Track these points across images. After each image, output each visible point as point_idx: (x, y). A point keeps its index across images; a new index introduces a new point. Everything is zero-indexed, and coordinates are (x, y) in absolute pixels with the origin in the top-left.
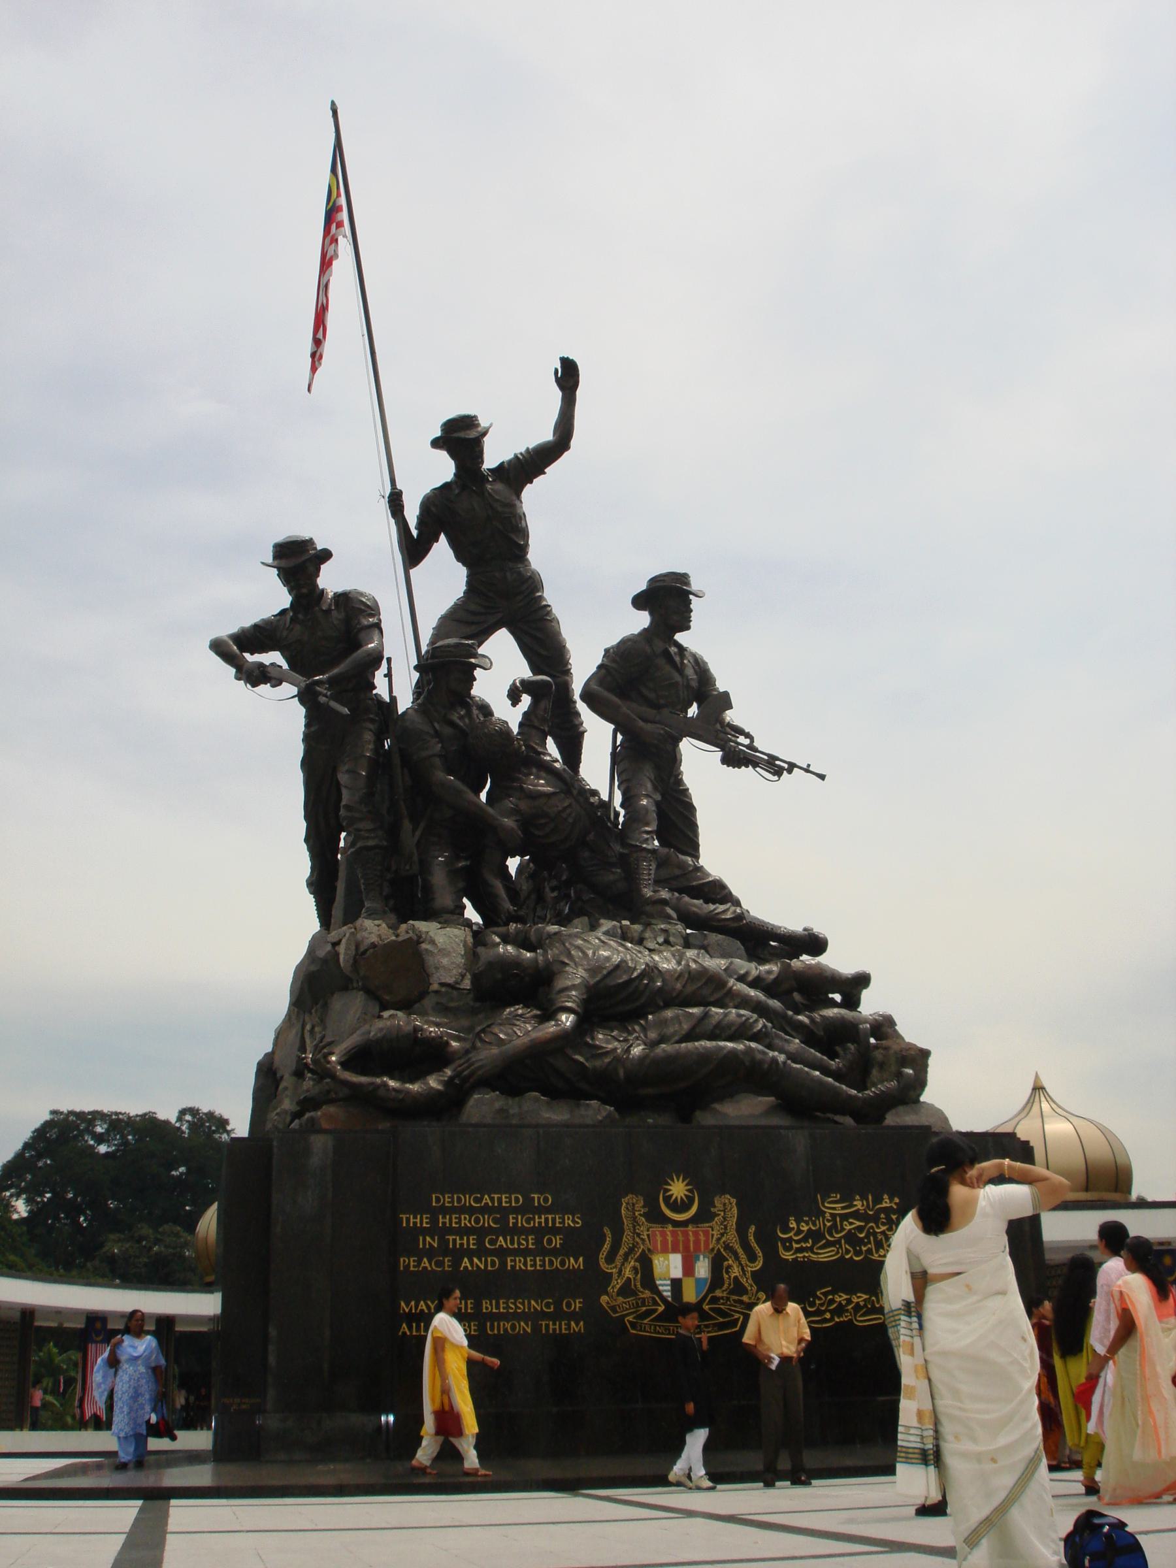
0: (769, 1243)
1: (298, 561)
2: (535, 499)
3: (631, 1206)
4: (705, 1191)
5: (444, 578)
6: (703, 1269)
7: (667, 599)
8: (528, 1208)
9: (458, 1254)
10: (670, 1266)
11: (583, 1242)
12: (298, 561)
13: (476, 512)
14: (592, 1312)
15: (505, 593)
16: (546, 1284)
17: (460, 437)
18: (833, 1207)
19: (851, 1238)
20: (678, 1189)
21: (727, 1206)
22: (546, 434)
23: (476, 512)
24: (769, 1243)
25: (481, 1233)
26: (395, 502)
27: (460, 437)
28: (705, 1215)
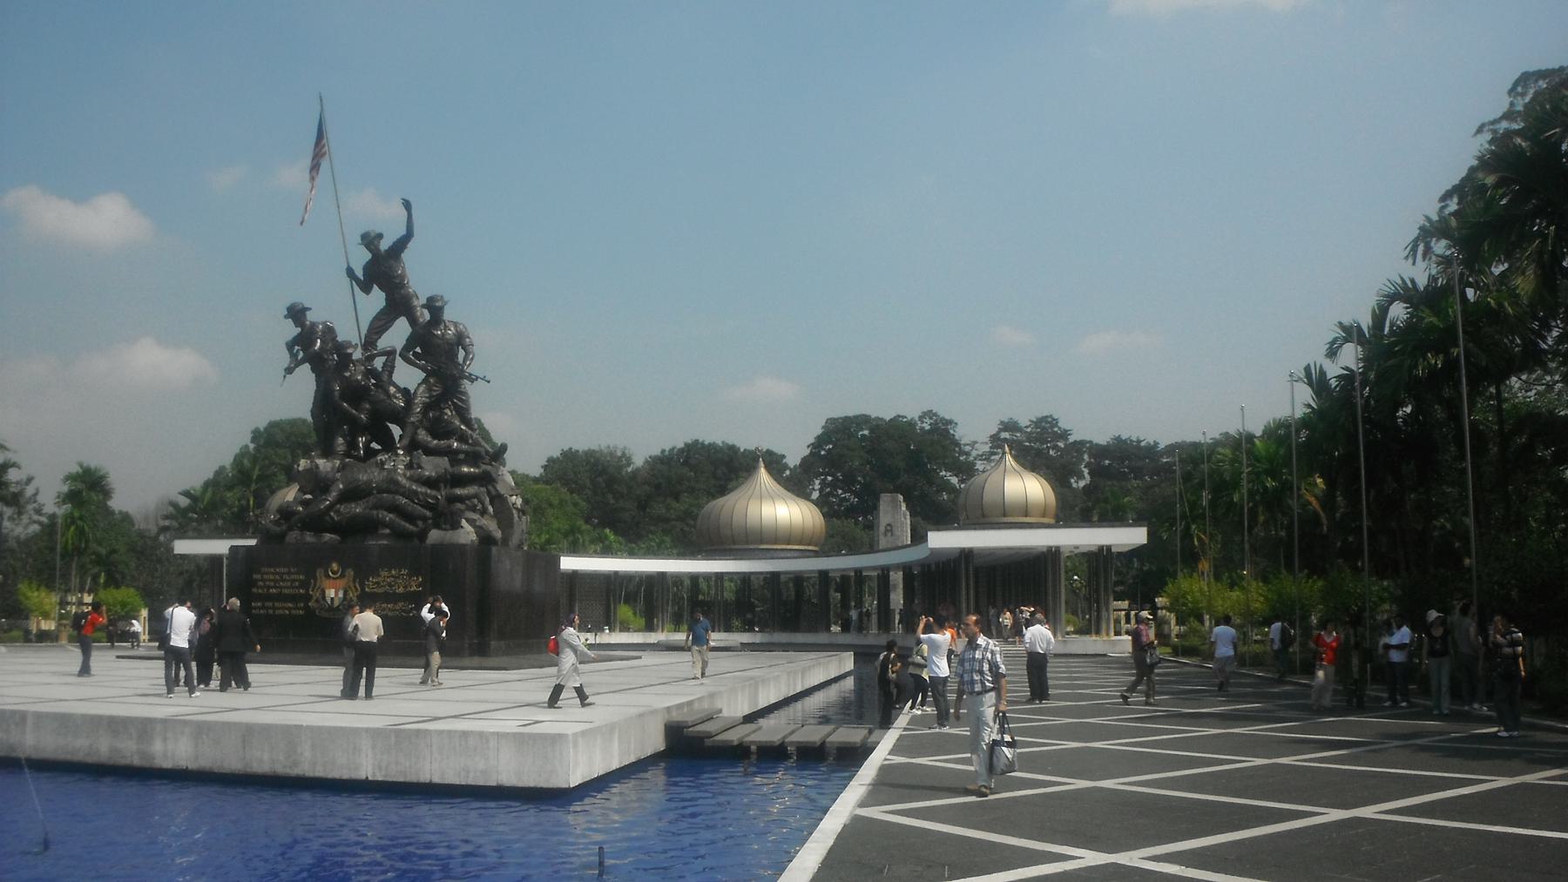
0: (362, 585)
1: (296, 313)
2: (405, 256)
3: (319, 573)
4: (344, 566)
5: (376, 300)
6: (341, 595)
7: (434, 306)
8: (289, 573)
9: (269, 587)
10: (331, 593)
11: (304, 585)
12: (296, 313)
13: (381, 269)
14: (306, 608)
15: (399, 304)
16: (293, 598)
17: (370, 241)
18: (384, 573)
19: (390, 585)
20: (335, 566)
21: (350, 572)
22: (403, 231)
23: (381, 269)
24: (362, 585)
25: (275, 581)
26: (350, 273)
27: (370, 241)
28: (343, 576)
